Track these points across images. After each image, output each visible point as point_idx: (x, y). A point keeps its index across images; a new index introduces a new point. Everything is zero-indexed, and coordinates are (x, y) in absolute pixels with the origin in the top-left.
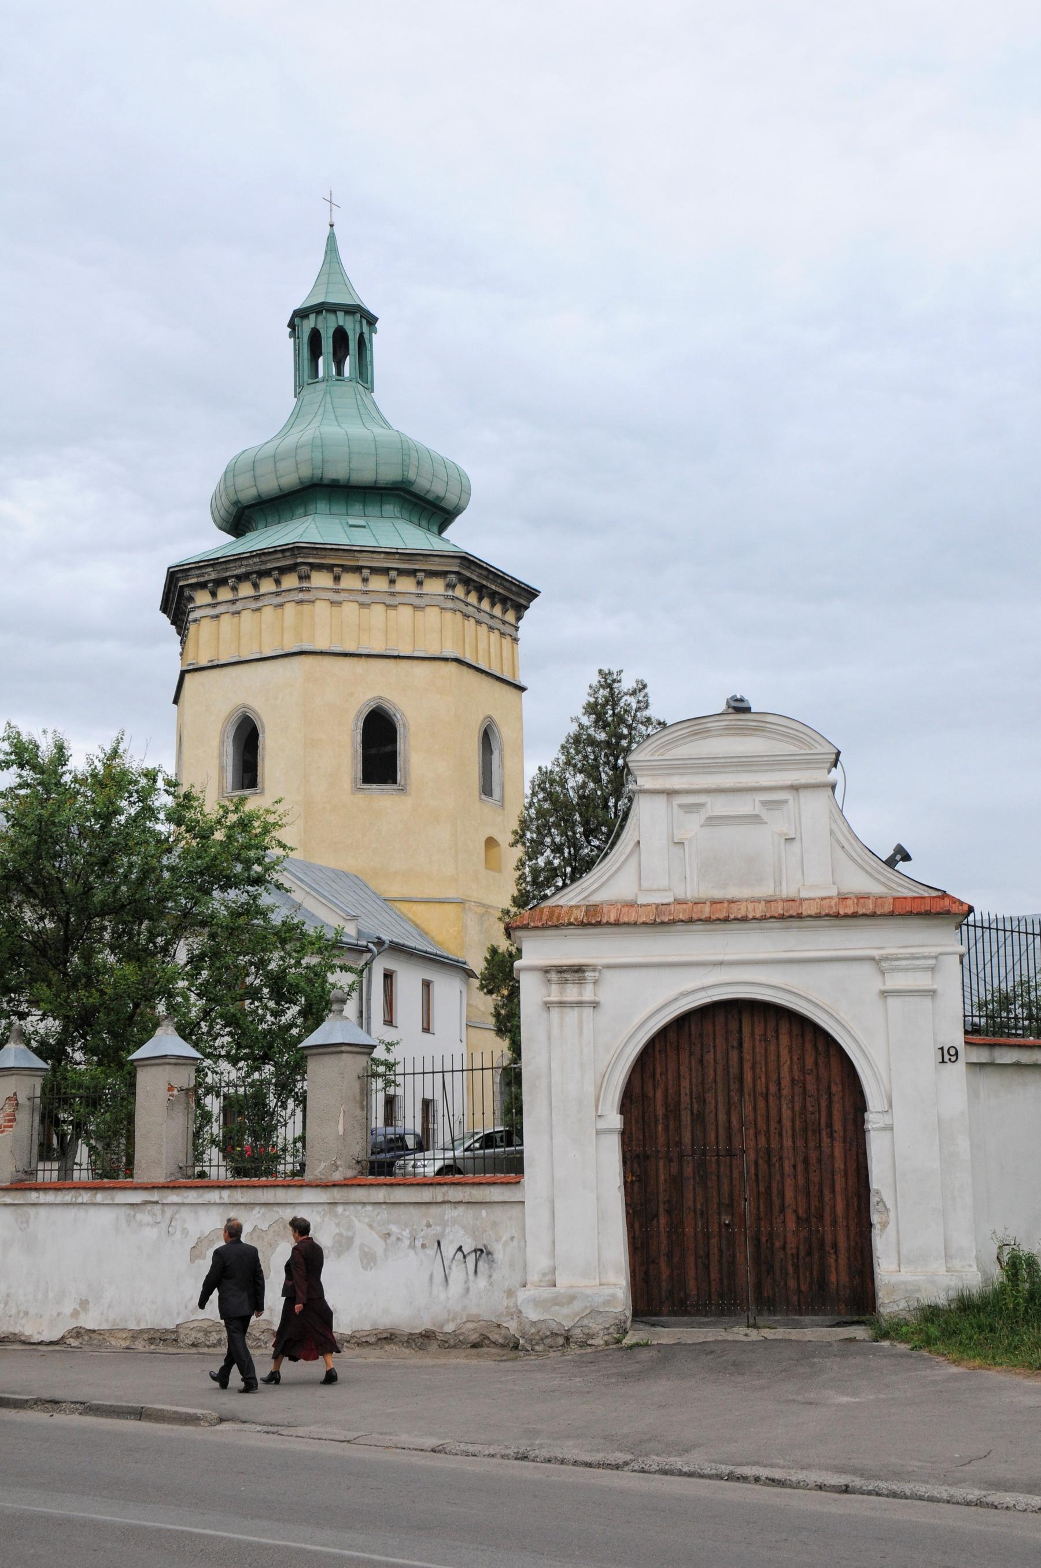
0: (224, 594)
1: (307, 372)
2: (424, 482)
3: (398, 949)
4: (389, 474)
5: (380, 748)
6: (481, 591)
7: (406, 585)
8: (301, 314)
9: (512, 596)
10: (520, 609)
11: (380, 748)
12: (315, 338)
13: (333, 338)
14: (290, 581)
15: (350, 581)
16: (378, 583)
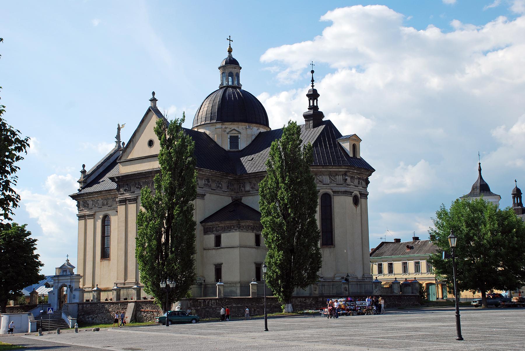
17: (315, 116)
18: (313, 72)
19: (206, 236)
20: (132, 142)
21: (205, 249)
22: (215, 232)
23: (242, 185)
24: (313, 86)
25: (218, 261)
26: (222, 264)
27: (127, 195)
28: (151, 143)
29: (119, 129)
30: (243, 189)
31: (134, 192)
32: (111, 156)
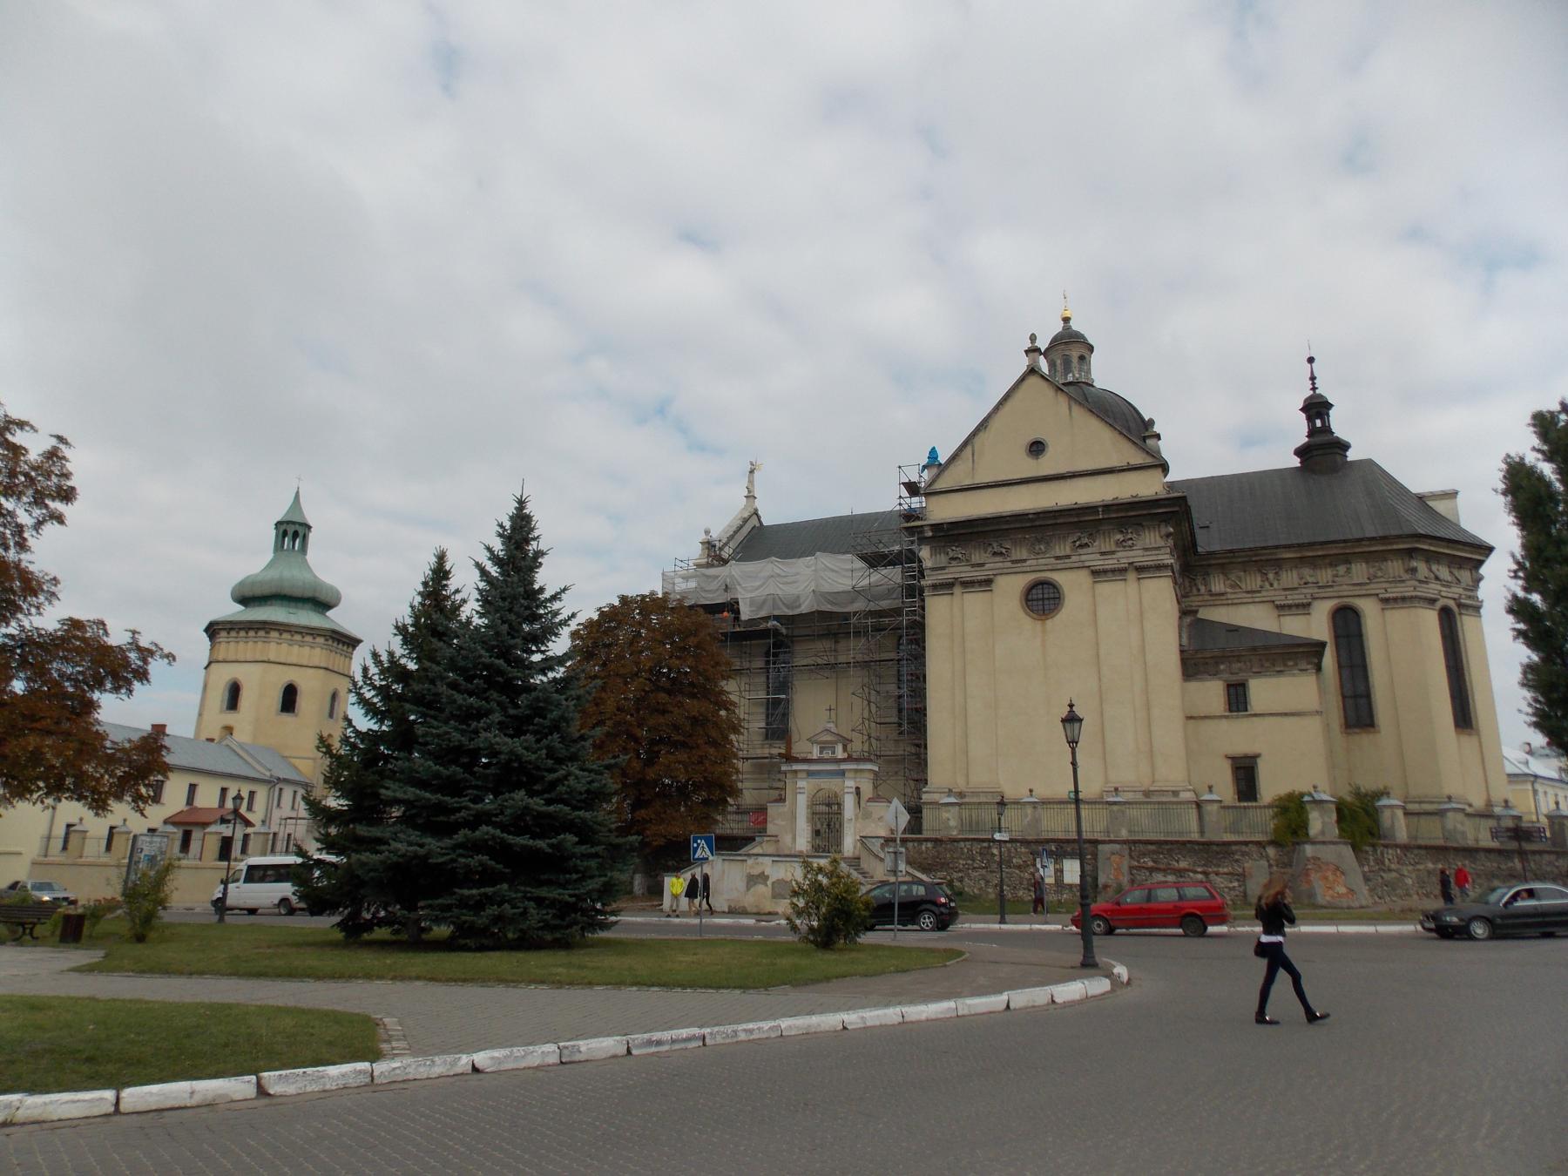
0: (233, 634)
1: (279, 546)
2: (322, 597)
3: (286, 781)
4: (309, 594)
5: (289, 700)
6: (339, 641)
7: (309, 639)
8: (278, 524)
9: (353, 642)
10: (354, 647)
11: (289, 700)
12: (285, 534)
13: (292, 532)
14: (261, 633)
15: (286, 636)
16: (298, 637)
17: (1322, 449)
18: (1311, 360)
19: (1193, 685)
20: (969, 448)
21: (1190, 718)
22: (1226, 676)
23: (1199, 581)
24: (1314, 389)
25: (1242, 748)
26: (1258, 756)
27: (965, 572)
28: (1037, 448)
29: (752, 472)
30: (1203, 589)
31: (982, 565)
32: (745, 521)
